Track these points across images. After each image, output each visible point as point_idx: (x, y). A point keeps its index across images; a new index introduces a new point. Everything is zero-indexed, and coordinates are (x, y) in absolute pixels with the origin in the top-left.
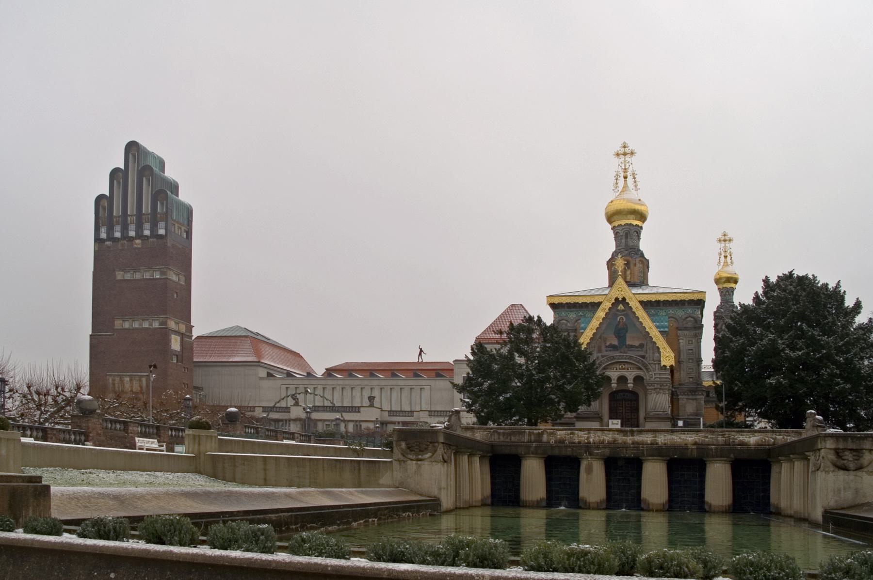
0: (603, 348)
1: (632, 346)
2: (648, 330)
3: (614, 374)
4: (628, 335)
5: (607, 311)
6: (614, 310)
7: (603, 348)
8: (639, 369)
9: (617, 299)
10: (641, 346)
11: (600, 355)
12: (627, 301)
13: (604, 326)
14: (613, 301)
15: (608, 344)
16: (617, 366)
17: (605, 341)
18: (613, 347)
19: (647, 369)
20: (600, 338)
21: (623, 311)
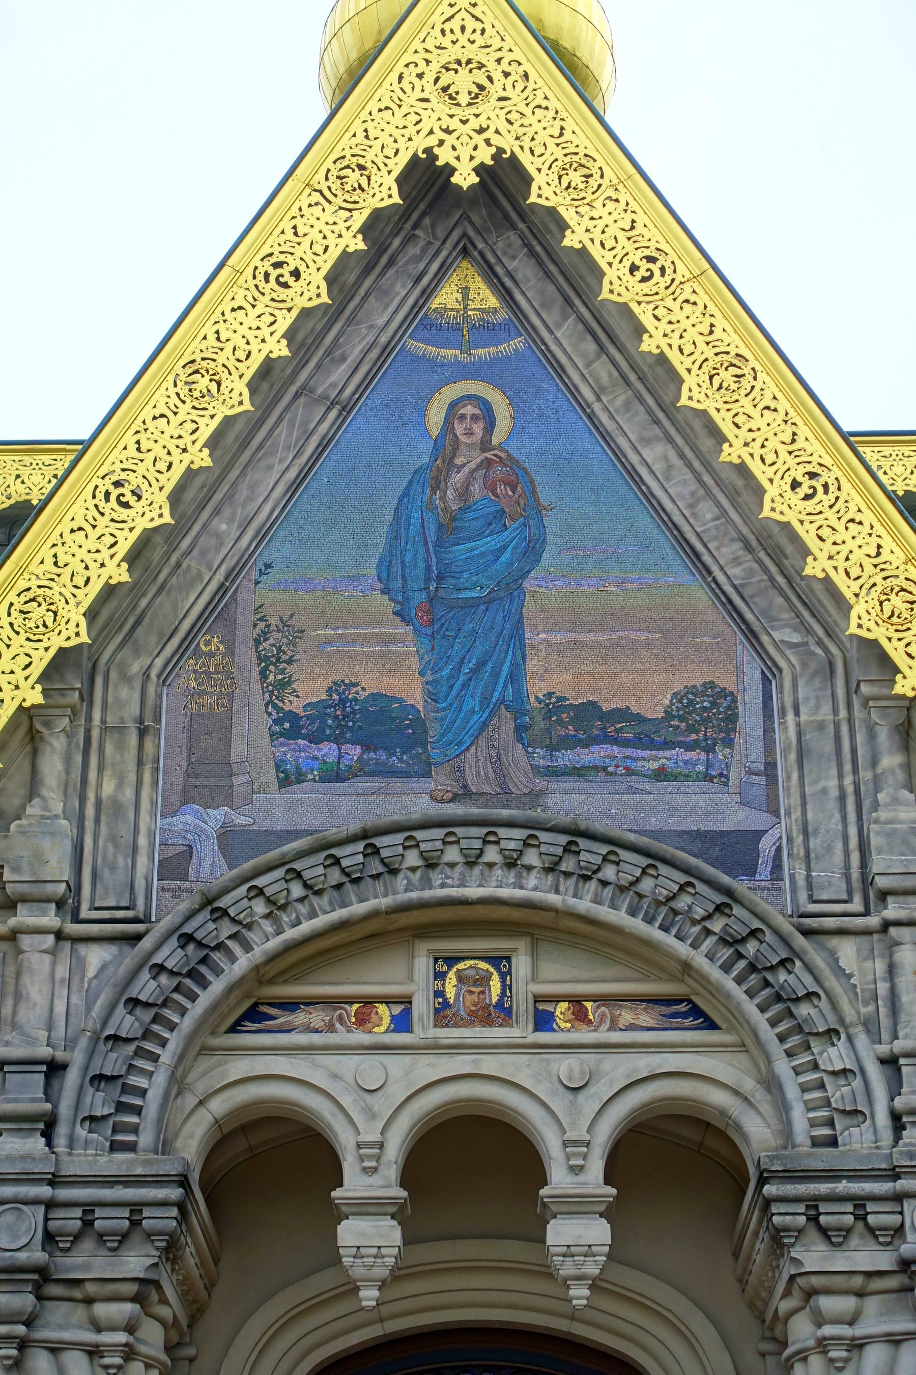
0: (252, 740)
1: (593, 723)
2: (780, 504)
3: (366, 1090)
4: (542, 591)
5: (312, 291)
6: (382, 316)
7: (252, 740)
8: (691, 1010)
9: (425, 180)
10: (705, 719)
11: (203, 823)
12: (544, 191)
13: (270, 480)
14: (385, 192)
15: (309, 689)
16: (412, 973)
17: (274, 665)
18: (370, 731)
19: (782, 1002)
20: (218, 611)
21: (486, 330)
